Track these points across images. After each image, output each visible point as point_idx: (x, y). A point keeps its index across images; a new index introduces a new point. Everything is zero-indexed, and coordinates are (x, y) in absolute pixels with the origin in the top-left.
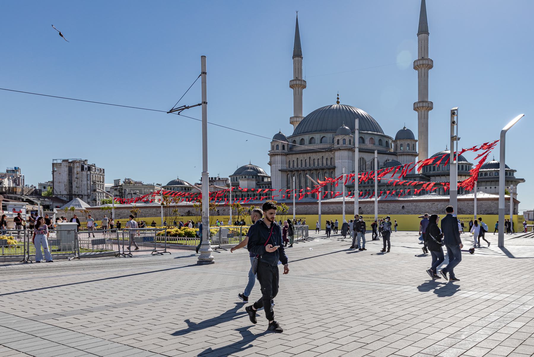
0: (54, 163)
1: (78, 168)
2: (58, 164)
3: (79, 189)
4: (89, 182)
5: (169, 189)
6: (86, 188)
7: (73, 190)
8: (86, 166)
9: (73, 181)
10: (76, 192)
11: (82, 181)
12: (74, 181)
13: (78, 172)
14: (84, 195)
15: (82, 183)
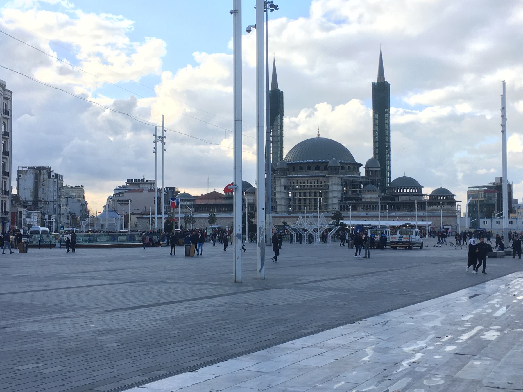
0: (19, 169)
1: (45, 176)
2: (24, 171)
3: (45, 195)
4: (55, 189)
5: (388, 228)
6: (52, 195)
7: (39, 196)
8: (52, 174)
9: (39, 187)
10: (42, 198)
11: (48, 188)
12: (40, 188)
13: (45, 179)
14: (51, 201)
15: (48, 190)
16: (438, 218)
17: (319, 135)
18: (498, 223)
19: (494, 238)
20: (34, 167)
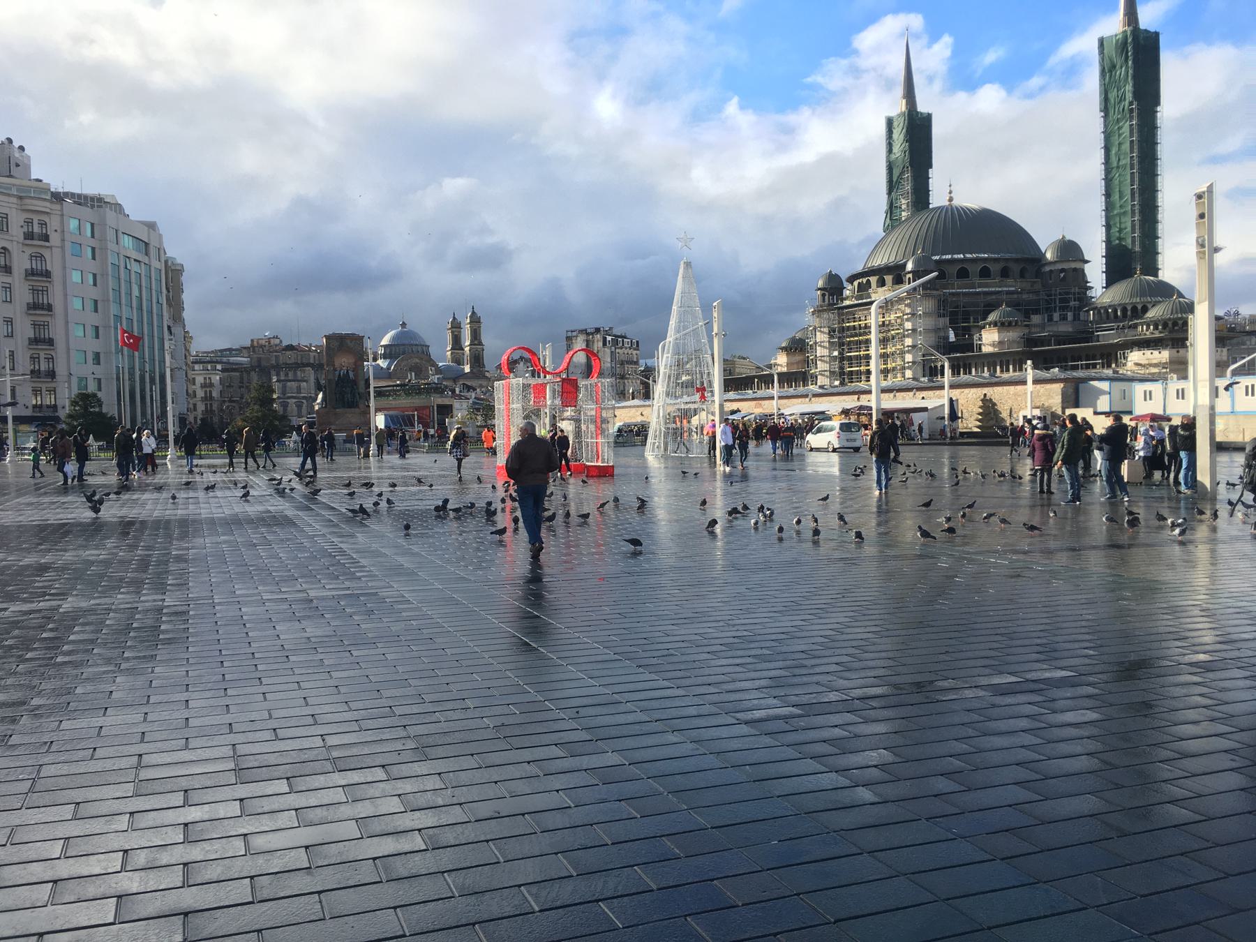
16: (1019, 388)
17: (951, 200)
18: (1181, 394)
19: (289, 454)
20: (586, 330)
